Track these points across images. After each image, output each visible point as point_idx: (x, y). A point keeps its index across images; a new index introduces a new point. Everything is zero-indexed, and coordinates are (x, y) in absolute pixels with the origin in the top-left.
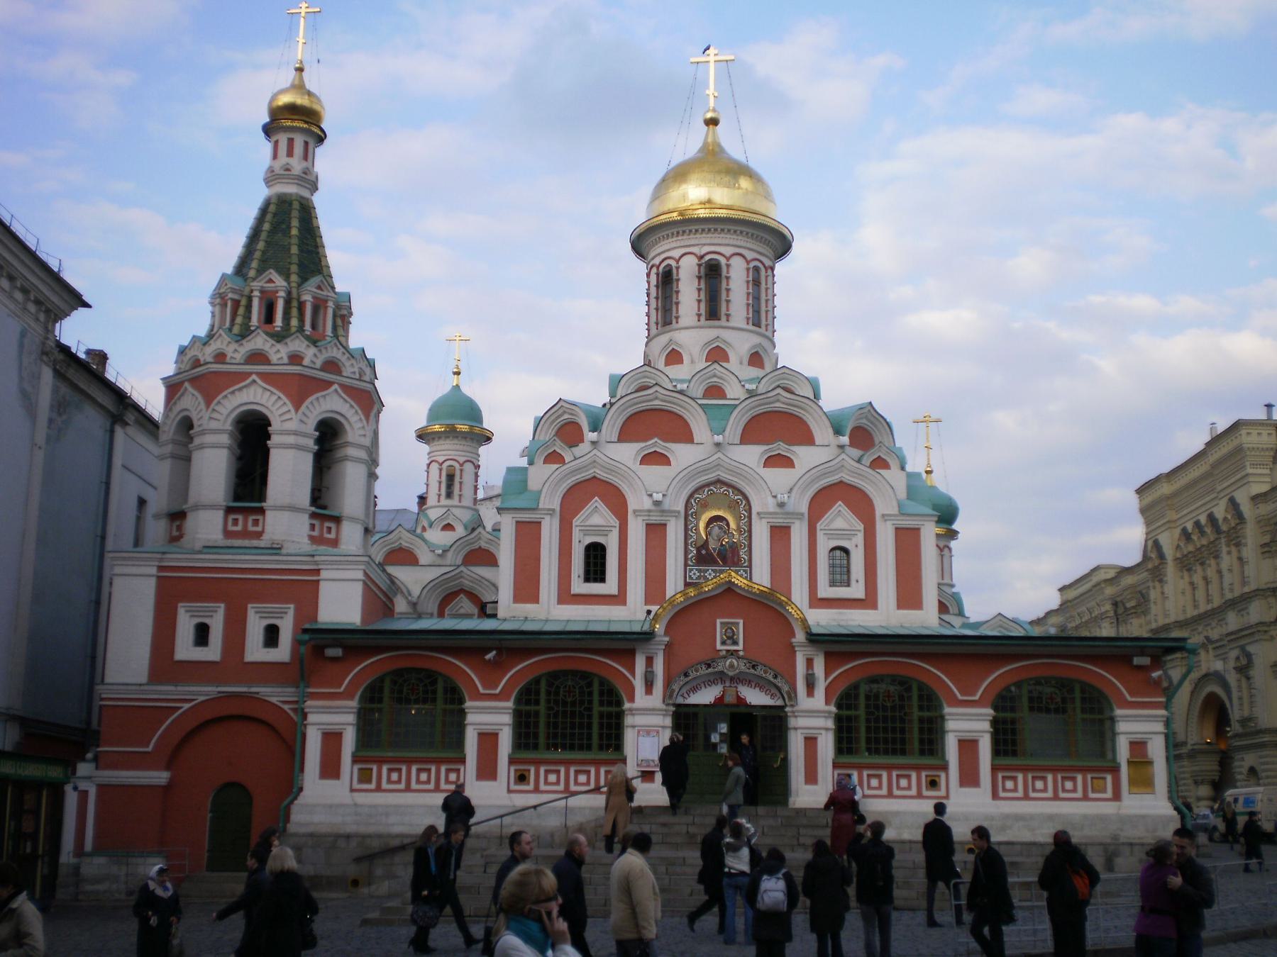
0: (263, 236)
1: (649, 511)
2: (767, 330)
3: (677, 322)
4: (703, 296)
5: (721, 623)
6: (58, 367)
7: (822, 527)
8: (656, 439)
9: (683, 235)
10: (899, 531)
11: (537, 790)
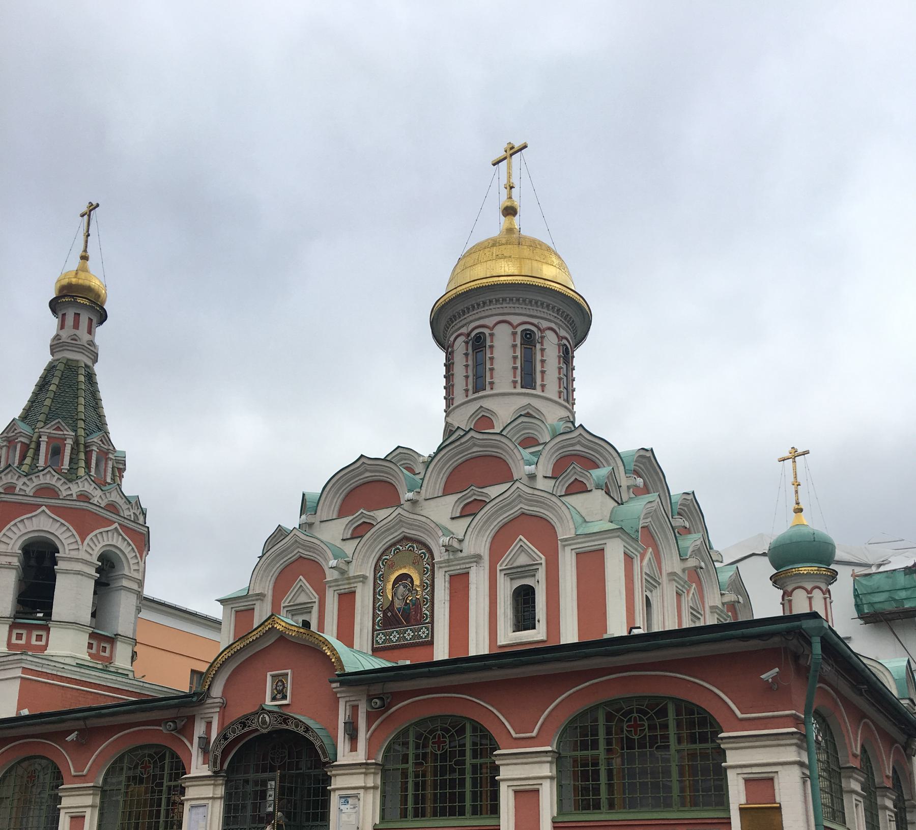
1: (336, 580)
2: (543, 391)
3: (452, 404)
4: (470, 373)
5: (273, 676)
7: (501, 568)
8: (362, 510)
9: (456, 320)
10: (580, 556)
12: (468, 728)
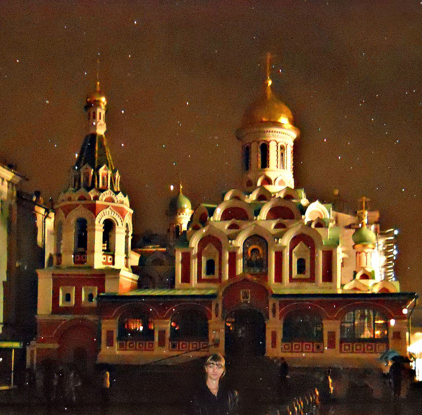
11: (179, 350)
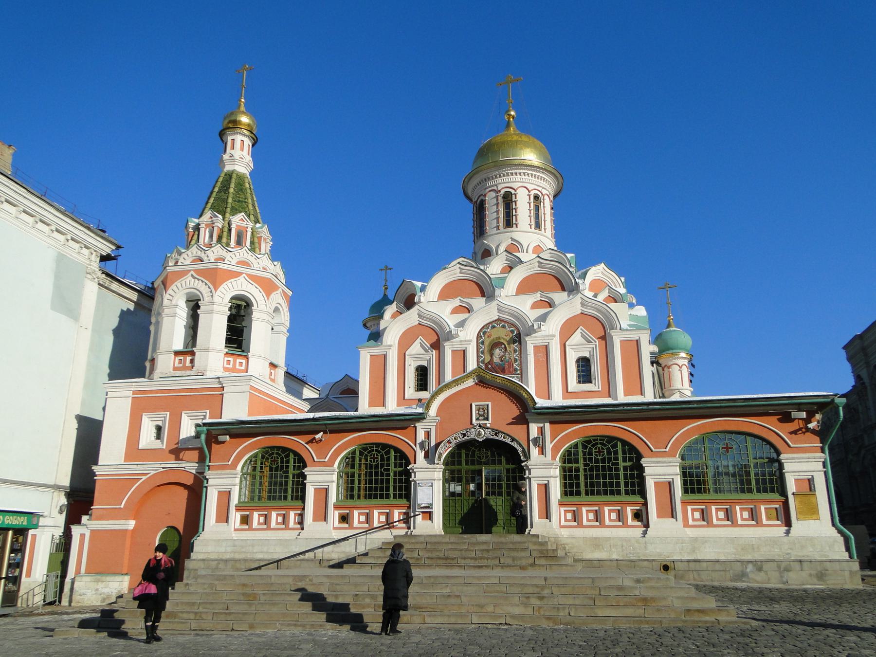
0: (214, 195)
2: (545, 232)
6: (101, 282)
8: (459, 298)
11: (351, 527)
12: (619, 444)
